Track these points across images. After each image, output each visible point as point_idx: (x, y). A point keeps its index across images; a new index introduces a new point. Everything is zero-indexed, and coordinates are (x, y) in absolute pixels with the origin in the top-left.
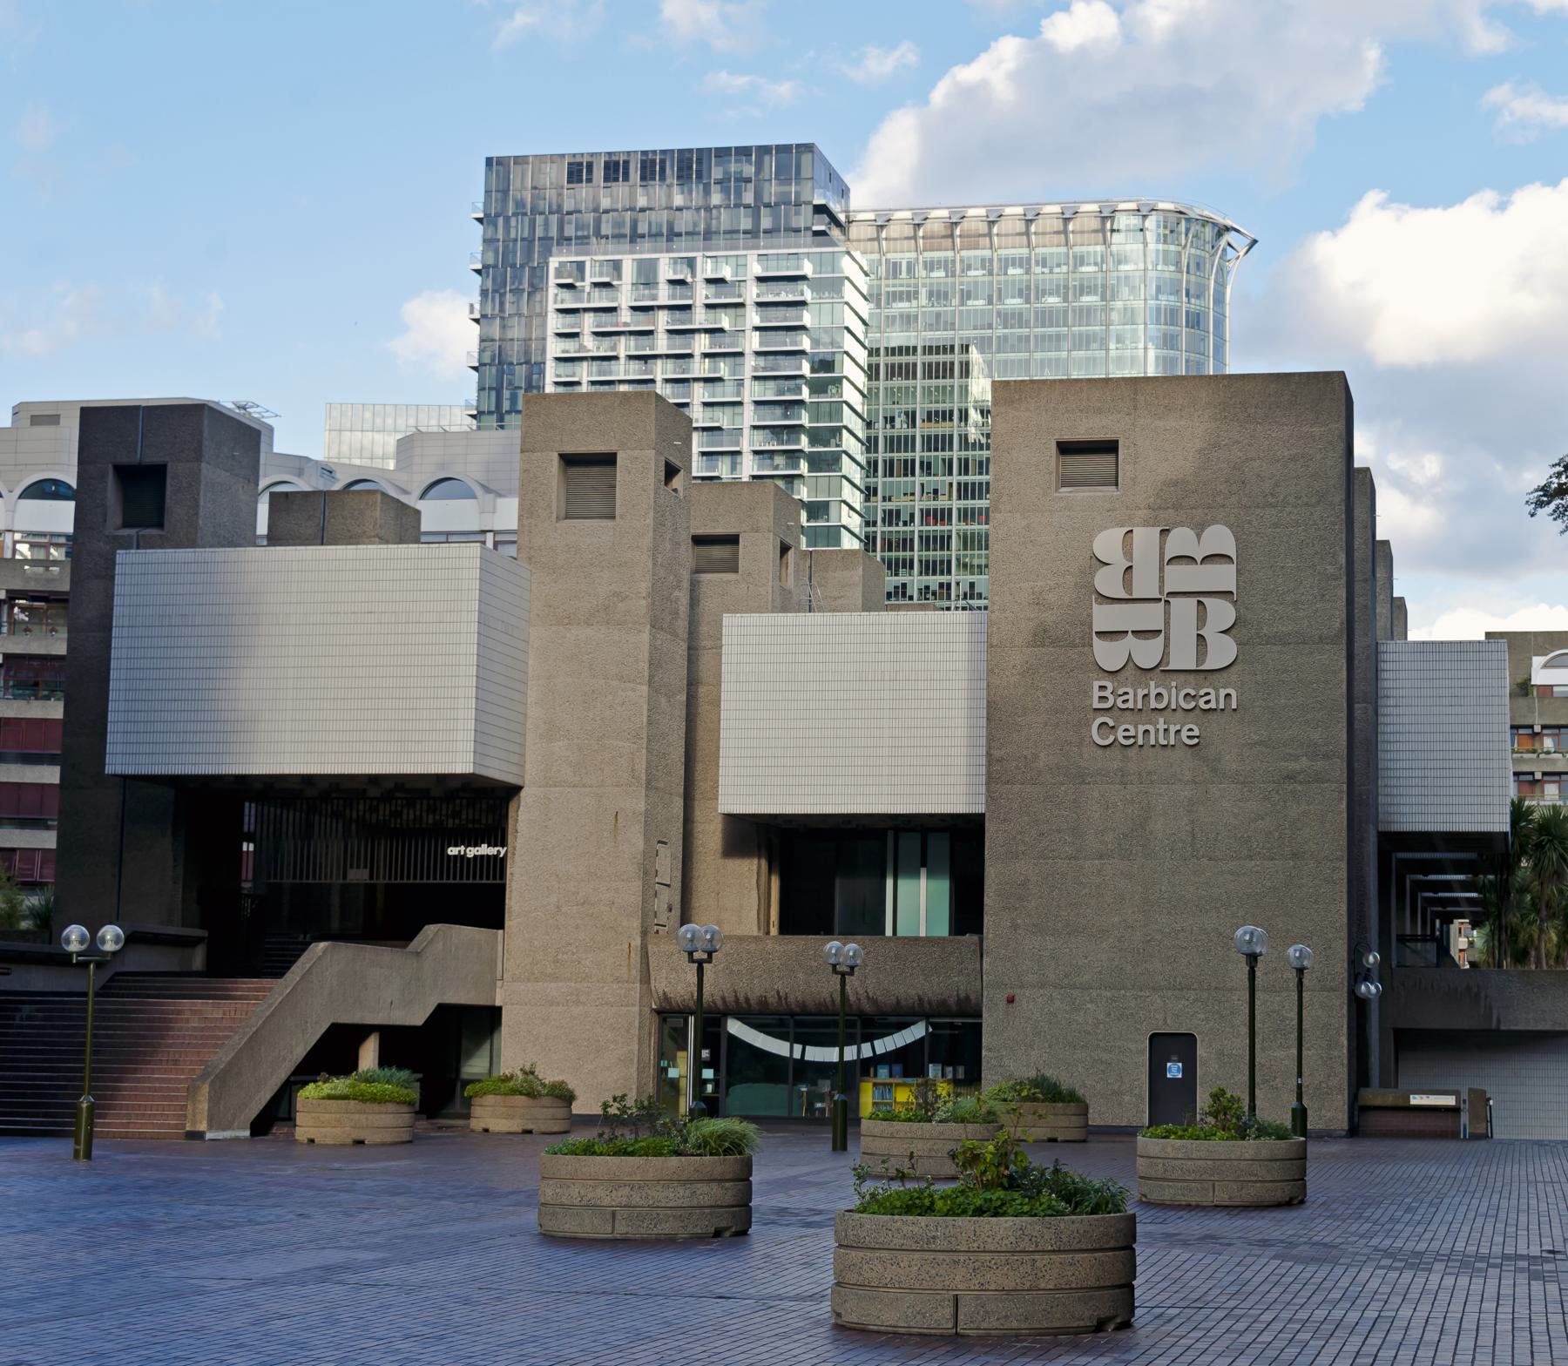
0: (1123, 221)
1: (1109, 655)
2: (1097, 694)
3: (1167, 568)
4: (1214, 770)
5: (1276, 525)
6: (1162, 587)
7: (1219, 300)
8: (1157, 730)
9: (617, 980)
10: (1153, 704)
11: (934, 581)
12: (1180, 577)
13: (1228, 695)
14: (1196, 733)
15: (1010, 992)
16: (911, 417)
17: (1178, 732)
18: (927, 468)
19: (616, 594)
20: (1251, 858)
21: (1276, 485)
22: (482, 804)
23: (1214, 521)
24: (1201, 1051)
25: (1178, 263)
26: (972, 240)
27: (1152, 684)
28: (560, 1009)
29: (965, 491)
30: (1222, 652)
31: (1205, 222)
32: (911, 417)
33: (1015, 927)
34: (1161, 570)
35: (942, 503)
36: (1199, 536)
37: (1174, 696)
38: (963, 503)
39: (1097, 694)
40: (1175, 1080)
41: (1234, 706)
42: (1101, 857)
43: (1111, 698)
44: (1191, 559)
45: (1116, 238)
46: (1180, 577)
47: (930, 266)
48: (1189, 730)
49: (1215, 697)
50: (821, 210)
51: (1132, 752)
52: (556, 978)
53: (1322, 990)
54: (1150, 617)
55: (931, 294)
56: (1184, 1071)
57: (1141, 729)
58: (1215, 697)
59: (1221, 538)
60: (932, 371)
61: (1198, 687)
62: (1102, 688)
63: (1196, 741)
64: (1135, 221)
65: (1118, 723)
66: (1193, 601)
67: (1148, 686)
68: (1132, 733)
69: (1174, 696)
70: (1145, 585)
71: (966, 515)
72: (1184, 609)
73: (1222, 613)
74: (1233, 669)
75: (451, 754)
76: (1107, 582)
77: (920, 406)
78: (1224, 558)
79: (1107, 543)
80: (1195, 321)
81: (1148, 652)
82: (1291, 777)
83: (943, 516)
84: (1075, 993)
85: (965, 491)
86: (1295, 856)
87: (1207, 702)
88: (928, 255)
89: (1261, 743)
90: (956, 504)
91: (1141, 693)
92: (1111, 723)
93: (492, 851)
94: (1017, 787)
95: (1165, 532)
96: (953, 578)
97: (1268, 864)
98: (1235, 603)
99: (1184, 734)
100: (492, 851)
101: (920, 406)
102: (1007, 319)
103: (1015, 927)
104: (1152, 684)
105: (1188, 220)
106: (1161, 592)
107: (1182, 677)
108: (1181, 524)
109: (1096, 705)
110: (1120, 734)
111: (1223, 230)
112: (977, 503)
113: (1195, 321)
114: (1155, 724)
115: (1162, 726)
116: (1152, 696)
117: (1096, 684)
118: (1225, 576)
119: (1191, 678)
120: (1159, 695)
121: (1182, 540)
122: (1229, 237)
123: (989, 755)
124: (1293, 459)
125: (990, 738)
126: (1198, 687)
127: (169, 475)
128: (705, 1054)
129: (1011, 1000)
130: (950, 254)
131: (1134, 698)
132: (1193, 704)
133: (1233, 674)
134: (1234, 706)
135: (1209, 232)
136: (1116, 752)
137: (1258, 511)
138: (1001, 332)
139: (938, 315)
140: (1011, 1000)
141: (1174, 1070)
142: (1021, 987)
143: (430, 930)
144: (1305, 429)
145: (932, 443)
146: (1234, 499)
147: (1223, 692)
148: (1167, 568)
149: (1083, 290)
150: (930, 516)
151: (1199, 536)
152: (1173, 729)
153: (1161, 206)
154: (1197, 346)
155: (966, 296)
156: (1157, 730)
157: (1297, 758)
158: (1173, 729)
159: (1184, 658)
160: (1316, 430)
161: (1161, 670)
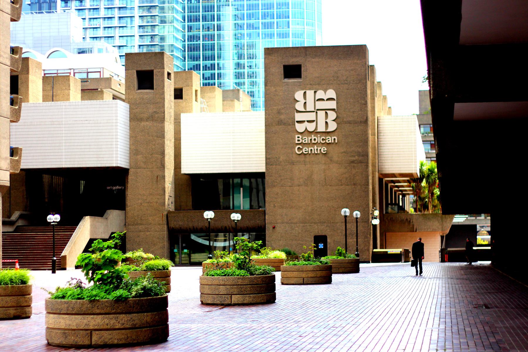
1: (300, 128)
2: (297, 139)
3: (317, 102)
4: (331, 160)
5: (347, 89)
6: (315, 108)
9: (159, 224)
10: (313, 142)
12: (320, 105)
13: (334, 139)
14: (326, 149)
15: (273, 225)
17: (320, 150)
19: (155, 112)
20: (342, 185)
21: (347, 77)
22: (118, 175)
23: (330, 88)
24: (328, 240)
28: (143, 233)
30: (333, 126)
33: (275, 206)
36: (325, 93)
37: (319, 139)
39: (297, 139)
40: (321, 249)
42: (299, 186)
43: (301, 140)
44: (323, 100)
46: (320, 105)
48: (324, 149)
51: (307, 156)
52: (141, 224)
53: (363, 222)
54: (312, 117)
56: (324, 246)
57: (310, 149)
62: (298, 137)
66: (324, 112)
67: (311, 136)
68: (307, 150)
69: (319, 139)
70: (310, 107)
72: (321, 114)
73: (332, 115)
74: (336, 131)
78: (332, 99)
79: (299, 95)
81: (311, 127)
82: (353, 162)
84: (292, 225)
86: (354, 184)
89: (344, 152)
91: (310, 138)
92: (301, 147)
93: (120, 188)
94: (274, 166)
95: (315, 92)
97: (347, 187)
98: (336, 112)
99: (322, 150)
100: (120, 188)
103: (275, 206)
104: (313, 136)
107: (321, 134)
108: (320, 89)
109: (297, 142)
110: (304, 150)
114: (314, 147)
115: (316, 148)
117: (297, 136)
118: (333, 105)
119: (324, 134)
120: (315, 139)
121: (320, 94)
123: (266, 157)
124: (352, 70)
125: (266, 152)
126: (325, 137)
127: (19, 78)
128: (184, 245)
129: (274, 228)
131: (307, 140)
133: (336, 133)
134: (336, 141)
136: (303, 156)
137: (342, 85)
140: (274, 228)
141: (321, 246)
142: (277, 223)
143: (109, 211)
144: (355, 61)
146: (335, 82)
147: (333, 138)
151: (325, 93)
152: (319, 149)
157: (354, 156)
158: (319, 149)
159: (321, 128)
160: (358, 61)
161: (315, 132)
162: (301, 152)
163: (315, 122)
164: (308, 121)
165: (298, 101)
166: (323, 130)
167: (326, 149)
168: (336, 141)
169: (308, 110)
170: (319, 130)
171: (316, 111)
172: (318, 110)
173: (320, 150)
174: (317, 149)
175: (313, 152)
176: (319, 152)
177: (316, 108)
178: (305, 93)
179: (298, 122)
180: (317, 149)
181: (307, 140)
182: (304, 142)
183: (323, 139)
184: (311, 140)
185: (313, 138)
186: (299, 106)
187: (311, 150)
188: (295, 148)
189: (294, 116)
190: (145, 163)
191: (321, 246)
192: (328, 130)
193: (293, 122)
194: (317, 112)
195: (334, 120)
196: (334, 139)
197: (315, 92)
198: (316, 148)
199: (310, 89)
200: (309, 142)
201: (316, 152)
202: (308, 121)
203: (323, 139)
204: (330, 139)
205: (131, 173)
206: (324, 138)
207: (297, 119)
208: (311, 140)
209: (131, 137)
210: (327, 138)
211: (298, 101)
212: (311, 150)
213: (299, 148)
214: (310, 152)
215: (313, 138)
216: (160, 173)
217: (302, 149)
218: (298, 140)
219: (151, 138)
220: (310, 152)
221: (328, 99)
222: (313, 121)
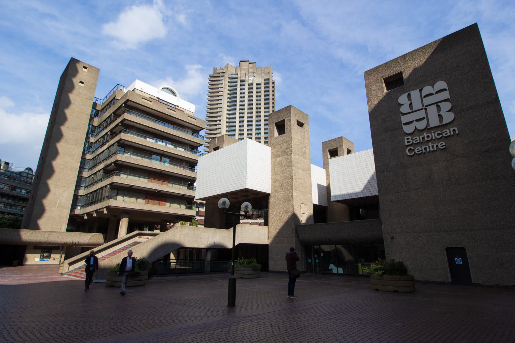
1: (408, 129)
2: (406, 141)
3: (424, 99)
8: (429, 147)
10: (426, 139)
13: (454, 130)
14: (444, 144)
17: (437, 146)
24: (468, 254)
27: (425, 133)
30: (449, 117)
34: (422, 101)
36: (433, 87)
37: (434, 135)
39: (406, 141)
40: (459, 265)
41: (457, 132)
48: (441, 144)
49: (448, 132)
57: (423, 148)
58: (448, 132)
59: (441, 84)
61: (441, 131)
62: (408, 139)
63: (444, 147)
65: (415, 148)
66: (435, 105)
67: (423, 134)
68: (420, 149)
69: (434, 135)
76: (403, 109)
79: (403, 99)
87: (447, 134)
91: (421, 137)
92: (412, 148)
95: (421, 90)
98: (450, 102)
99: (439, 146)
104: (425, 133)
106: (423, 106)
109: (407, 144)
110: (416, 151)
116: (426, 137)
117: (406, 138)
118: (446, 95)
119: (439, 129)
120: (428, 137)
121: (427, 90)
126: (441, 131)
129: (392, 238)
131: (418, 139)
132: (441, 136)
140: (392, 238)
141: (458, 261)
147: (451, 130)
148: (424, 99)
151: (433, 87)
152: (435, 145)
156: (429, 147)
158: (435, 145)
159: (434, 122)
161: (428, 129)
162: (413, 153)
163: (426, 119)
164: (416, 121)
165: (402, 105)
166: (438, 123)
167: (444, 144)
168: (457, 132)
169: (414, 110)
170: (431, 126)
171: (425, 108)
172: (426, 106)
173: (437, 146)
174: (433, 146)
175: (428, 150)
176: (435, 149)
177: (425, 105)
178: (409, 95)
179: (405, 124)
180: (433, 146)
181: (418, 139)
182: (414, 142)
183: (438, 134)
184: (423, 138)
185: (426, 135)
186: (405, 109)
187: (425, 148)
188: (406, 151)
189: (401, 120)
190: (280, 188)
191: (458, 261)
192: (444, 123)
193: (400, 126)
194: (426, 109)
195: (449, 111)
196: (454, 130)
197: (421, 90)
198: (430, 145)
199: (414, 89)
200: (421, 141)
201: (432, 150)
202: (416, 121)
203: (438, 134)
204: (448, 132)
205: (271, 196)
206: (440, 132)
207: (403, 122)
208: (423, 138)
209: (272, 170)
210: (444, 131)
211: (402, 105)
212: (425, 148)
213: (410, 150)
214: (424, 151)
215: (426, 135)
216: (290, 194)
217: (414, 150)
218: (409, 142)
219: (284, 168)
220: (424, 151)
221: (437, 92)
222: (423, 118)
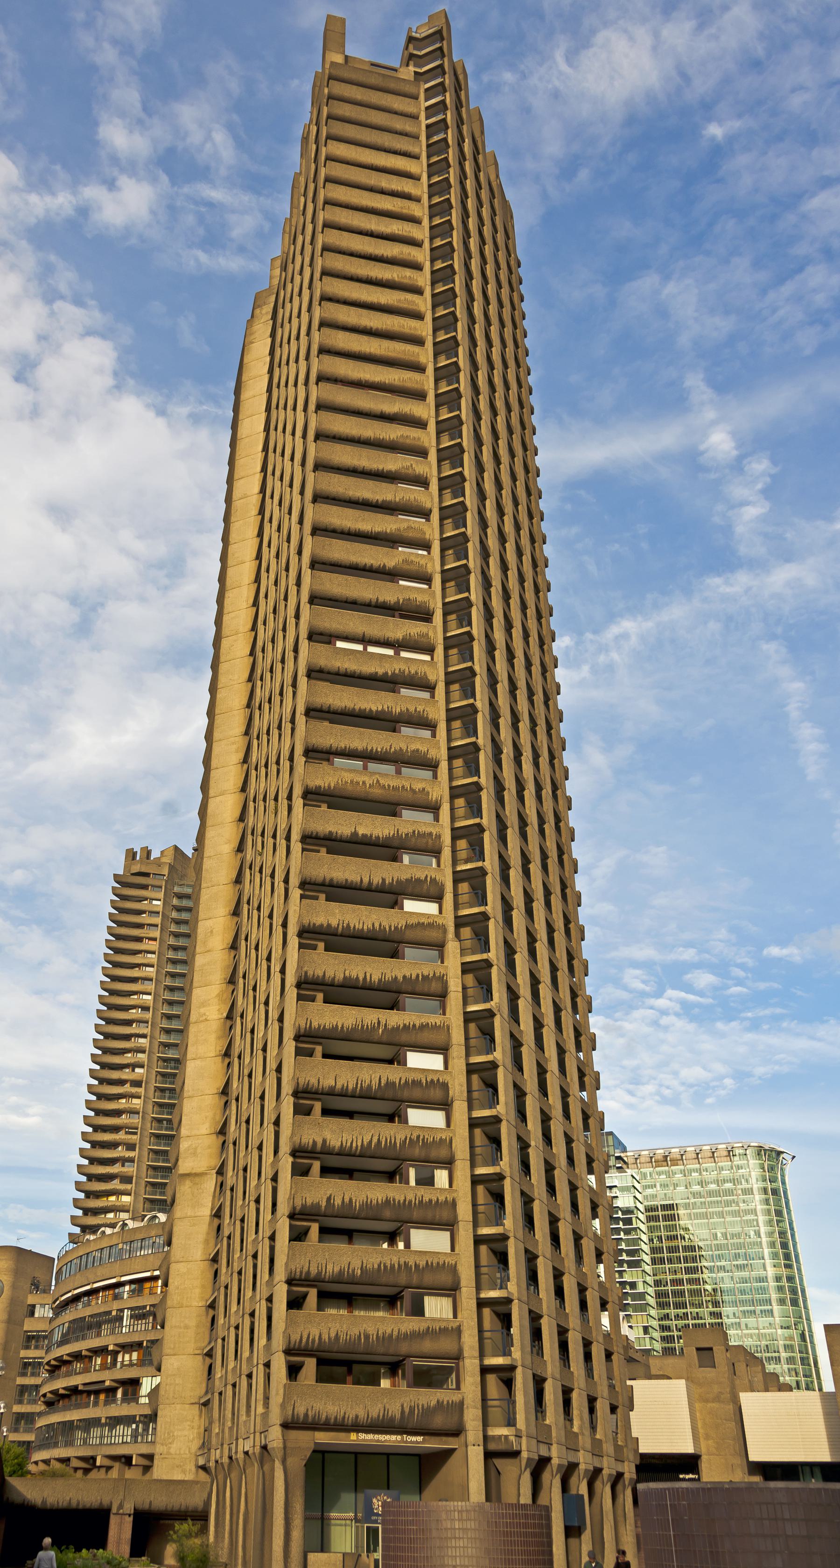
0: (737, 1152)
7: (784, 1183)
11: (681, 1311)
16: (660, 1239)
18: (670, 1261)
25: (763, 1168)
26: (675, 1162)
29: (688, 1271)
31: (772, 1150)
32: (660, 1239)
35: (679, 1276)
38: (688, 1276)
45: (736, 1158)
47: (659, 1174)
50: (619, 1158)
55: (661, 1185)
60: (666, 1218)
64: (742, 1151)
71: (690, 1281)
75: (688, 1448)
77: (664, 1234)
80: (775, 1192)
83: (680, 1282)
85: (688, 1271)
88: (658, 1169)
90: (685, 1277)
96: (689, 1310)
101: (664, 1234)
102: (694, 1195)
105: (765, 1150)
111: (779, 1153)
112: (694, 1276)
113: (775, 1192)
122: (784, 1155)
130: (667, 1168)
135: (774, 1154)
138: (693, 1200)
139: (665, 1194)
145: (671, 1250)
149: (724, 1181)
150: (675, 1282)
153: (752, 1144)
154: (777, 1203)
155: (676, 1185)
